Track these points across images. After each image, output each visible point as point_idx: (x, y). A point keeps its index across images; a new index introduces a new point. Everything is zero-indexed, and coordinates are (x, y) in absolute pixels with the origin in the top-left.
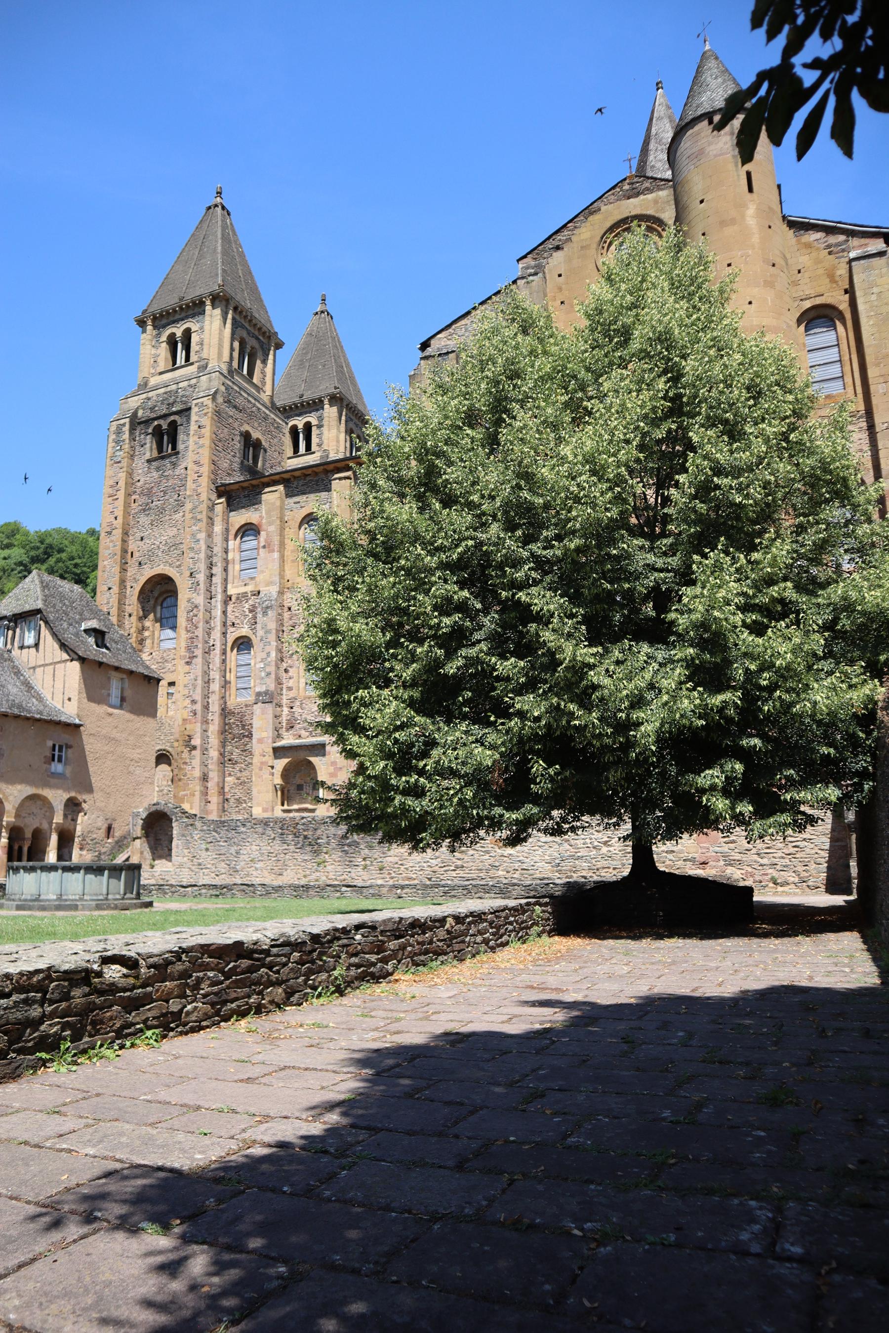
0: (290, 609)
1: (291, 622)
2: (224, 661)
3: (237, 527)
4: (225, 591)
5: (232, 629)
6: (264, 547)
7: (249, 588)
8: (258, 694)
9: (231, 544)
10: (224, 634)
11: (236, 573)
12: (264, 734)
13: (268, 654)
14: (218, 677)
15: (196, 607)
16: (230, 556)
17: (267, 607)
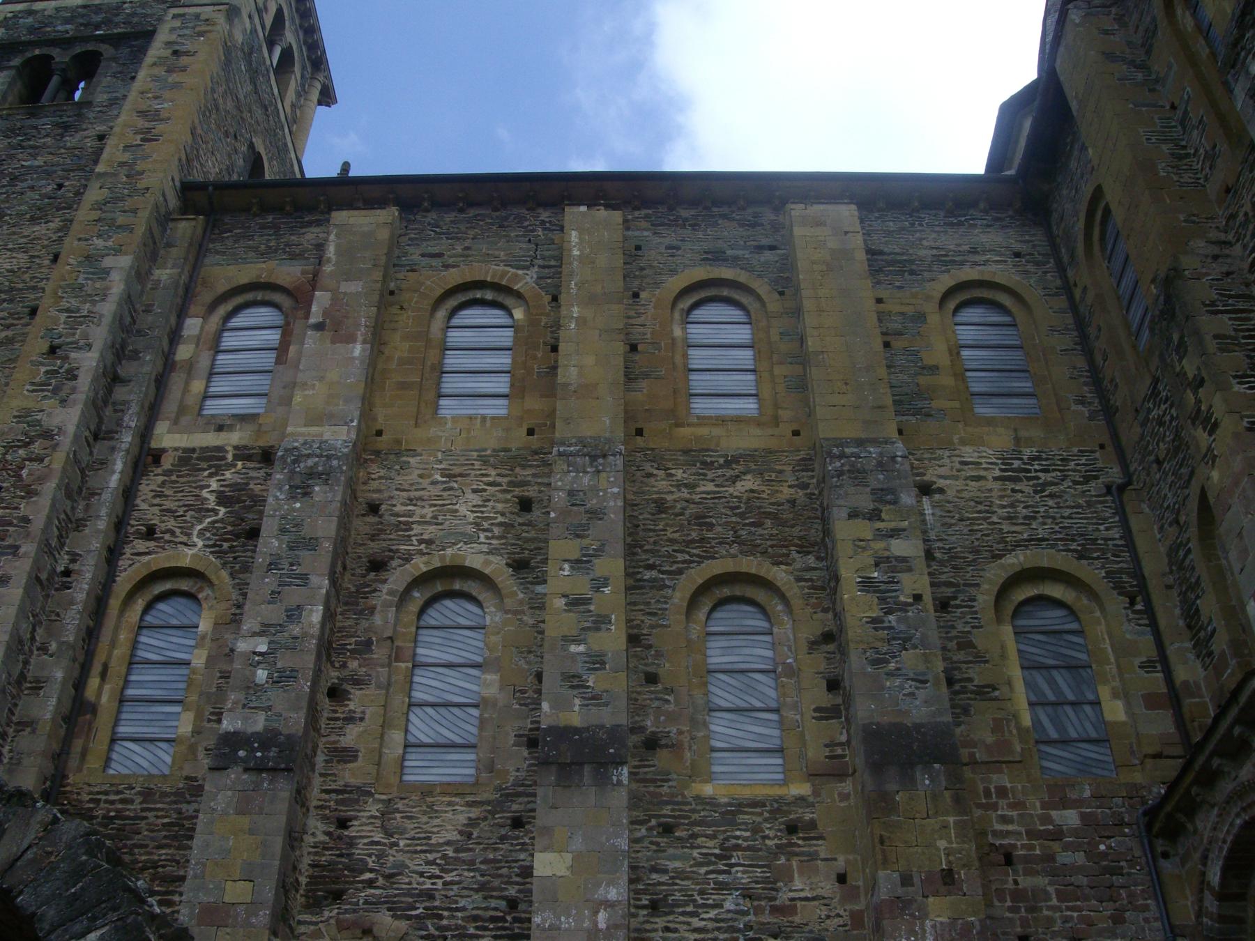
0: (374, 509)
1: (374, 547)
2: (91, 635)
3: (222, 287)
4: (145, 433)
5: (141, 545)
6: (319, 327)
7: (234, 438)
8: (232, 741)
9: (192, 325)
10: (113, 554)
11: (191, 400)
12: (237, 892)
13: (294, 614)
14: (59, 675)
15: (47, 435)
16: (184, 352)
17: (312, 474)
